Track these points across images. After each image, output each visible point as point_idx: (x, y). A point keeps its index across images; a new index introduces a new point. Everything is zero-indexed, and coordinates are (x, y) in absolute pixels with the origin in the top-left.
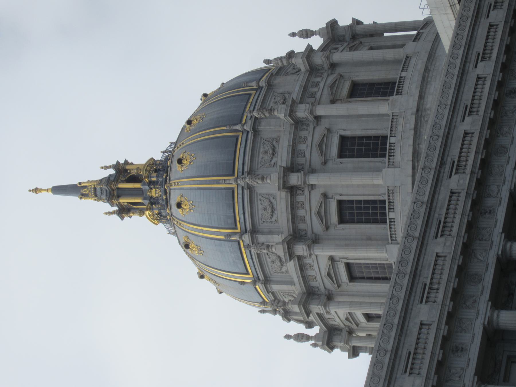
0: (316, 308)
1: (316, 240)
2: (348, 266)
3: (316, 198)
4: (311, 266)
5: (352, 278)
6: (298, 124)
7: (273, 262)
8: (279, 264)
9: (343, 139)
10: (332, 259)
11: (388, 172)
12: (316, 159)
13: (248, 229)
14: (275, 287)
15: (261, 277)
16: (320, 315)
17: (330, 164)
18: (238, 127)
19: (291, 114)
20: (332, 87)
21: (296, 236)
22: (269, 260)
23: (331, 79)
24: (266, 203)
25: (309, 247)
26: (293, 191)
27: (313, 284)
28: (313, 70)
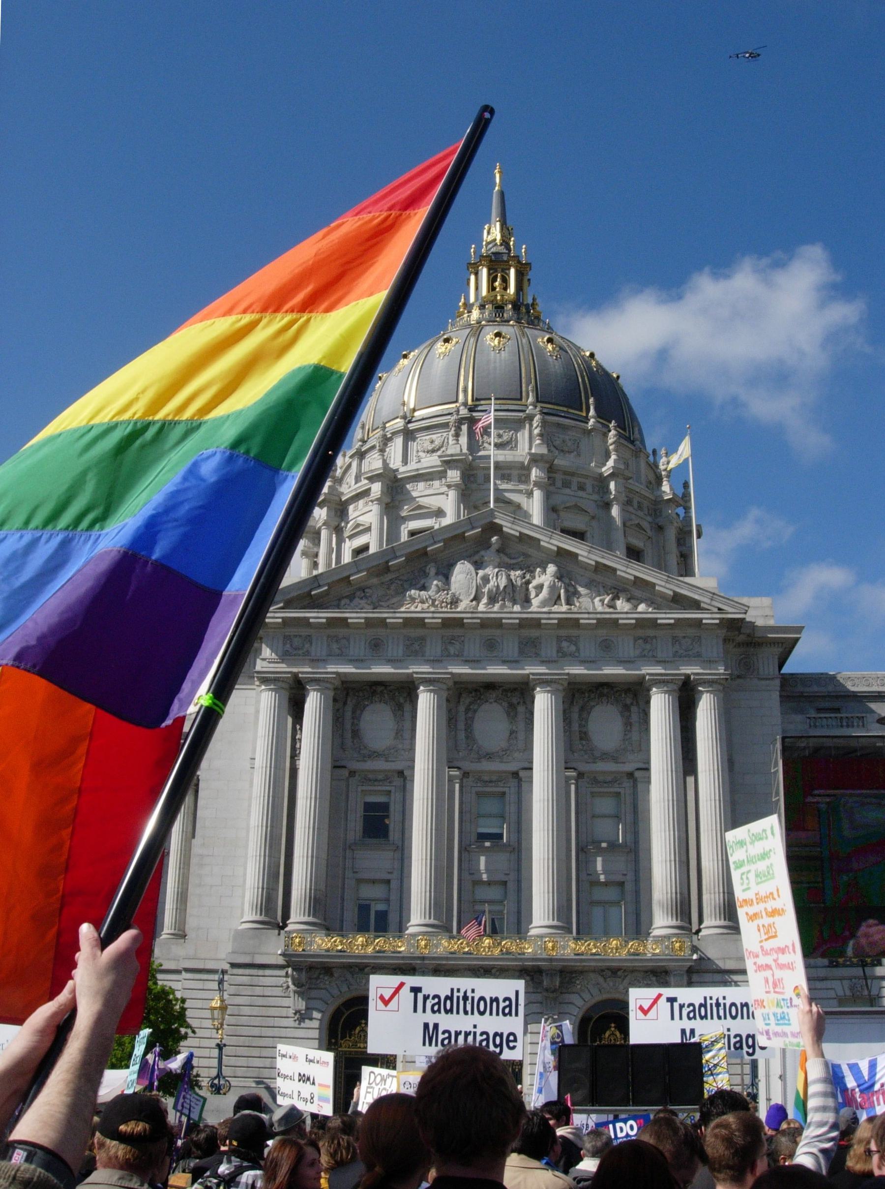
0: (376, 488)
7: (432, 442)
8: (430, 448)
12: (558, 500)
13: (474, 414)
14: (399, 441)
15: (411, 426)
16: (366, 493)
17: (554, 515)
18: (592, 412)
20: (638, 526)
22: (434, 437)
23: (645, 525)
24: (506, 437)
25: (457, 486)
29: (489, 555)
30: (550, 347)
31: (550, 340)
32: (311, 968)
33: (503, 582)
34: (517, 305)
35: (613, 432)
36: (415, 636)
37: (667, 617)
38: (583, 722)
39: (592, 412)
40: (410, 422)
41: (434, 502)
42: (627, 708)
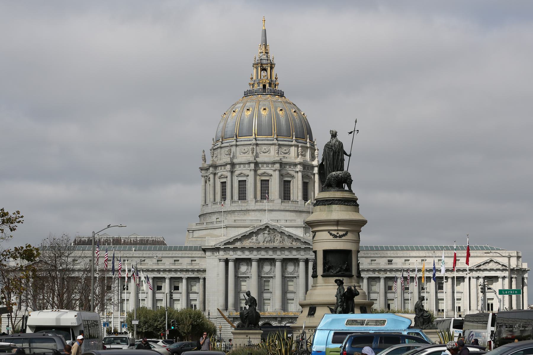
1: (255, 171)
2: (246, 181)
3: (270, 172)
4: (245, 167)
5: (239, 181)
6: (295, 165)
9: (290, 181)
10: (248, 176)
11: (280, 201)
12: (284, 172)
15: (238, 143)
18: (294, 138)
19: (300, 164)
21: (256, 164)
23: (309, 174)
24: (267, 150)
26: (274, 163)
27: (237, 166)
28: (313, 167)
29: (266, 232)
30: (281, 112)
31: (281, 110)
32: (234, 318)
33: (269, 239)
34: (270, 84)
35: (300, 148)
36: (251, 249)
37: (303, 246)
38: (286, 266)
39: (294, 138)
40: (237, 141)
41: (247, 172)
42: (295, 263)
